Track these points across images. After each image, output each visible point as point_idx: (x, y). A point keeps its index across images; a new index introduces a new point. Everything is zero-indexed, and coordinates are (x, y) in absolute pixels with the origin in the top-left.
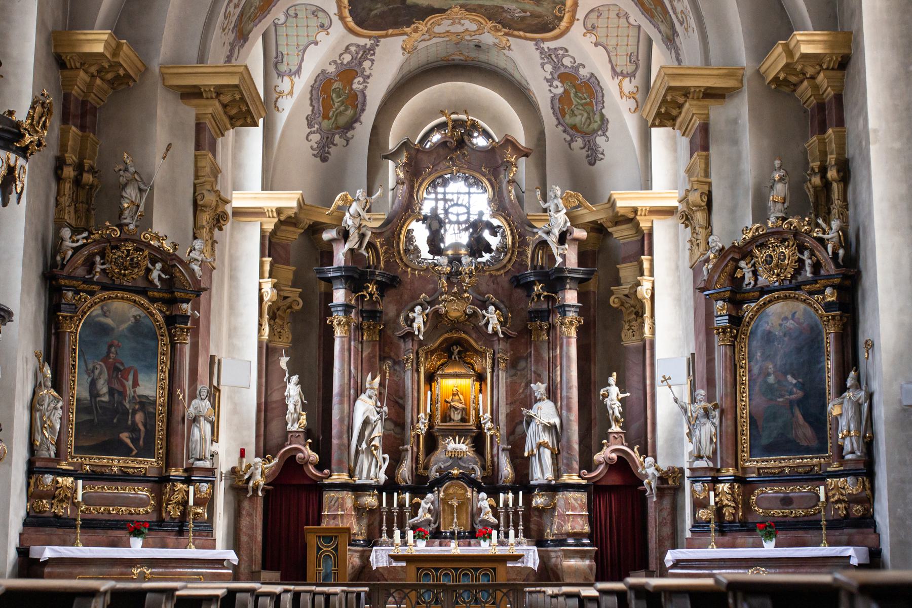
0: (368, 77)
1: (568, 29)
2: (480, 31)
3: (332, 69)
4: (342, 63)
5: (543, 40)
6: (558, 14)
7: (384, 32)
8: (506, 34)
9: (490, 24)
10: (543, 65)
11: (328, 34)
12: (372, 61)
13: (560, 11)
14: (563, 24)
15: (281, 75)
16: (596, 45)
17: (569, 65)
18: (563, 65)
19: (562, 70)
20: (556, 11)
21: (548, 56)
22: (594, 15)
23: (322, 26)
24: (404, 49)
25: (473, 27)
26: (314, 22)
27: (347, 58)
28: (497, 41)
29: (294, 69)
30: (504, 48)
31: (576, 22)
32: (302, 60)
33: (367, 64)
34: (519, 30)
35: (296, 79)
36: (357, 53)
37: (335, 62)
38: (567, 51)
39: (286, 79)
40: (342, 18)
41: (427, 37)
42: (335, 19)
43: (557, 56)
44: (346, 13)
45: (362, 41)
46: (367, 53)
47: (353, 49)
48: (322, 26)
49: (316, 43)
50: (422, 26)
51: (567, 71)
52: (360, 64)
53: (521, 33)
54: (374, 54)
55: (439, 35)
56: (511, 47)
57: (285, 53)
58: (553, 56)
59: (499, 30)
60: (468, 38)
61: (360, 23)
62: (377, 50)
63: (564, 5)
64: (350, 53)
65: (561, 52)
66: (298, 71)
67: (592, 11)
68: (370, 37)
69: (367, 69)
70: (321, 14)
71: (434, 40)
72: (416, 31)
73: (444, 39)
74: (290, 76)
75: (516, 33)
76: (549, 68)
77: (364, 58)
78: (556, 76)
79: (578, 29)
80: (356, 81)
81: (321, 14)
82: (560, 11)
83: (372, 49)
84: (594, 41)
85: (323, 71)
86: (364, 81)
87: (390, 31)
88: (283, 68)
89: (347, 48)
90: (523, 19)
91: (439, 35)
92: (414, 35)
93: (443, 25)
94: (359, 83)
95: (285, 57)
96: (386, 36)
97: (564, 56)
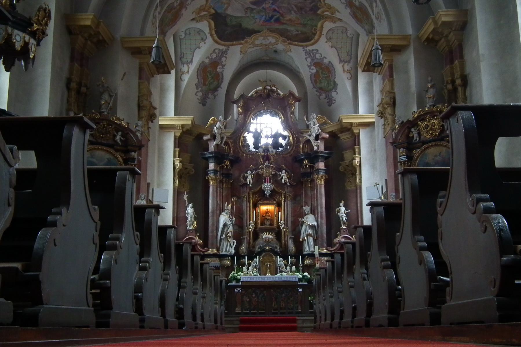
0: (224, 65)
1: (318, 39)
2: (276, 43)
3: (207, 61)
4: (212, 58)
5: (307, 46)
6: (314, 32)
7: (231, 43)
8: (289, 44)
9: (281, 39)
10: (306, 59)
11: (205, 43)
12: (226, 58)
13: (315, 30)
14: (316, 37)
15: (183, 64)
16: (332, 47)
17: (319, 58)
18: (316, 58)
19: (316, 61)
20: (313, 30)
21: (309, 54)
22: (331, 32)
23: (202, 39)
24: (241, 52)
25: (273, 40)
26: (198, 37)
27: (214, 56)
28: (285, 47)
29: (190, 60)
30: (288, 51)
31: (322, 36)
32: (193, 56)
33: (223, 59)
34: (295, 41)
35: (190, 66)
36: (219, 53)
37: (208, 57)
38: (318, 51)
39: (185, 65)
40: (211, 35)
41: (251, 46)
42: (208, 35)
43: (313, 54)
44: (214, 32)
45: (221, 47)
46: (223, 53)
47: (217, 51)
48: (202, 39)
49: (200, 48)
50: (249, 40)
51: (317, 61)
52: (220, 59)
53: (296, 43)
54: (227, 54)
55: (257, 45)
56: (292, 50)
57: (185, 53)
58: (311, 54)
59: (285, 42)
60: (271, 47)
61: (220, 38)
62: (229, 52)
63: (317, 27)
64: (216, 53)
65: (315, 52)
66: (191, 62)
67: (330, 30)
68: (225, 45)
69: (224, 62)
70: (201, 33)
71: (256, 48)
72: (246, 42)
73: (260, 47)
74: (187, 64)
75: (294, 43)
76: (309, 60)
77: (222, 56)
78: (312, 64)
79: (323, 39)
80: (218, 67)
81: (201, 33)
82: (315, 30)
83: (226, 51)
84: (331, 45)
85: (203, 62)
86: (223, 68)
87: (235, 42)
88: (184, 60)
89: (214, 50)
90: (297, 35)
91: (257, 45)
92: (246, 45)
93: (259, 40)
94: (220, 68)
95: (185, 54)
96: (233, 45)
97: (316, 53)
